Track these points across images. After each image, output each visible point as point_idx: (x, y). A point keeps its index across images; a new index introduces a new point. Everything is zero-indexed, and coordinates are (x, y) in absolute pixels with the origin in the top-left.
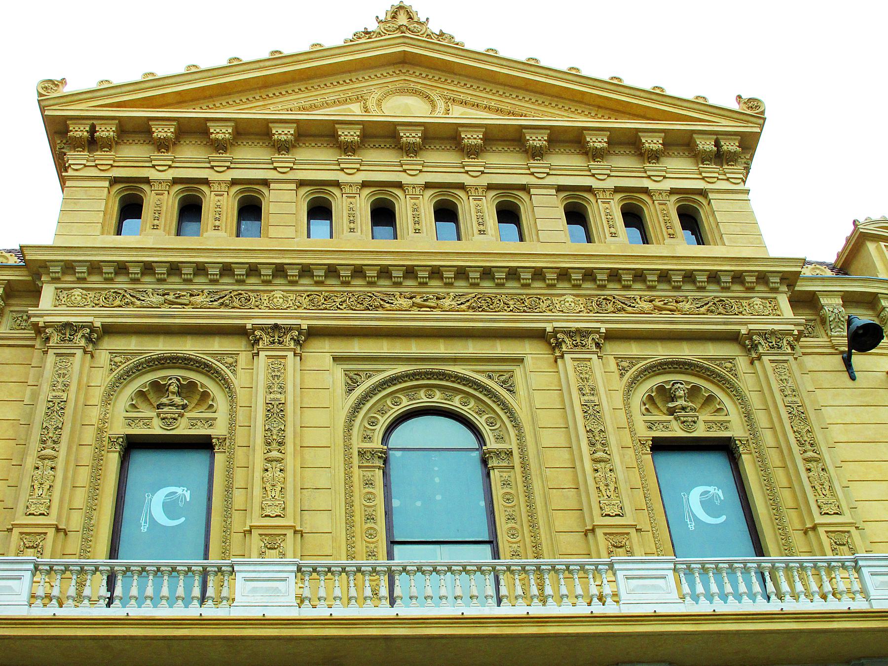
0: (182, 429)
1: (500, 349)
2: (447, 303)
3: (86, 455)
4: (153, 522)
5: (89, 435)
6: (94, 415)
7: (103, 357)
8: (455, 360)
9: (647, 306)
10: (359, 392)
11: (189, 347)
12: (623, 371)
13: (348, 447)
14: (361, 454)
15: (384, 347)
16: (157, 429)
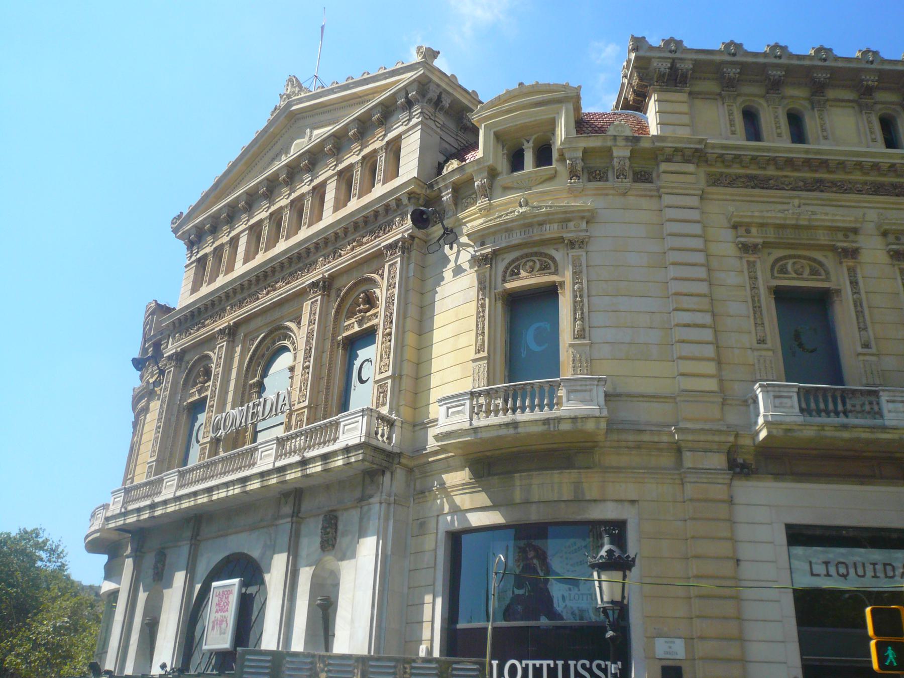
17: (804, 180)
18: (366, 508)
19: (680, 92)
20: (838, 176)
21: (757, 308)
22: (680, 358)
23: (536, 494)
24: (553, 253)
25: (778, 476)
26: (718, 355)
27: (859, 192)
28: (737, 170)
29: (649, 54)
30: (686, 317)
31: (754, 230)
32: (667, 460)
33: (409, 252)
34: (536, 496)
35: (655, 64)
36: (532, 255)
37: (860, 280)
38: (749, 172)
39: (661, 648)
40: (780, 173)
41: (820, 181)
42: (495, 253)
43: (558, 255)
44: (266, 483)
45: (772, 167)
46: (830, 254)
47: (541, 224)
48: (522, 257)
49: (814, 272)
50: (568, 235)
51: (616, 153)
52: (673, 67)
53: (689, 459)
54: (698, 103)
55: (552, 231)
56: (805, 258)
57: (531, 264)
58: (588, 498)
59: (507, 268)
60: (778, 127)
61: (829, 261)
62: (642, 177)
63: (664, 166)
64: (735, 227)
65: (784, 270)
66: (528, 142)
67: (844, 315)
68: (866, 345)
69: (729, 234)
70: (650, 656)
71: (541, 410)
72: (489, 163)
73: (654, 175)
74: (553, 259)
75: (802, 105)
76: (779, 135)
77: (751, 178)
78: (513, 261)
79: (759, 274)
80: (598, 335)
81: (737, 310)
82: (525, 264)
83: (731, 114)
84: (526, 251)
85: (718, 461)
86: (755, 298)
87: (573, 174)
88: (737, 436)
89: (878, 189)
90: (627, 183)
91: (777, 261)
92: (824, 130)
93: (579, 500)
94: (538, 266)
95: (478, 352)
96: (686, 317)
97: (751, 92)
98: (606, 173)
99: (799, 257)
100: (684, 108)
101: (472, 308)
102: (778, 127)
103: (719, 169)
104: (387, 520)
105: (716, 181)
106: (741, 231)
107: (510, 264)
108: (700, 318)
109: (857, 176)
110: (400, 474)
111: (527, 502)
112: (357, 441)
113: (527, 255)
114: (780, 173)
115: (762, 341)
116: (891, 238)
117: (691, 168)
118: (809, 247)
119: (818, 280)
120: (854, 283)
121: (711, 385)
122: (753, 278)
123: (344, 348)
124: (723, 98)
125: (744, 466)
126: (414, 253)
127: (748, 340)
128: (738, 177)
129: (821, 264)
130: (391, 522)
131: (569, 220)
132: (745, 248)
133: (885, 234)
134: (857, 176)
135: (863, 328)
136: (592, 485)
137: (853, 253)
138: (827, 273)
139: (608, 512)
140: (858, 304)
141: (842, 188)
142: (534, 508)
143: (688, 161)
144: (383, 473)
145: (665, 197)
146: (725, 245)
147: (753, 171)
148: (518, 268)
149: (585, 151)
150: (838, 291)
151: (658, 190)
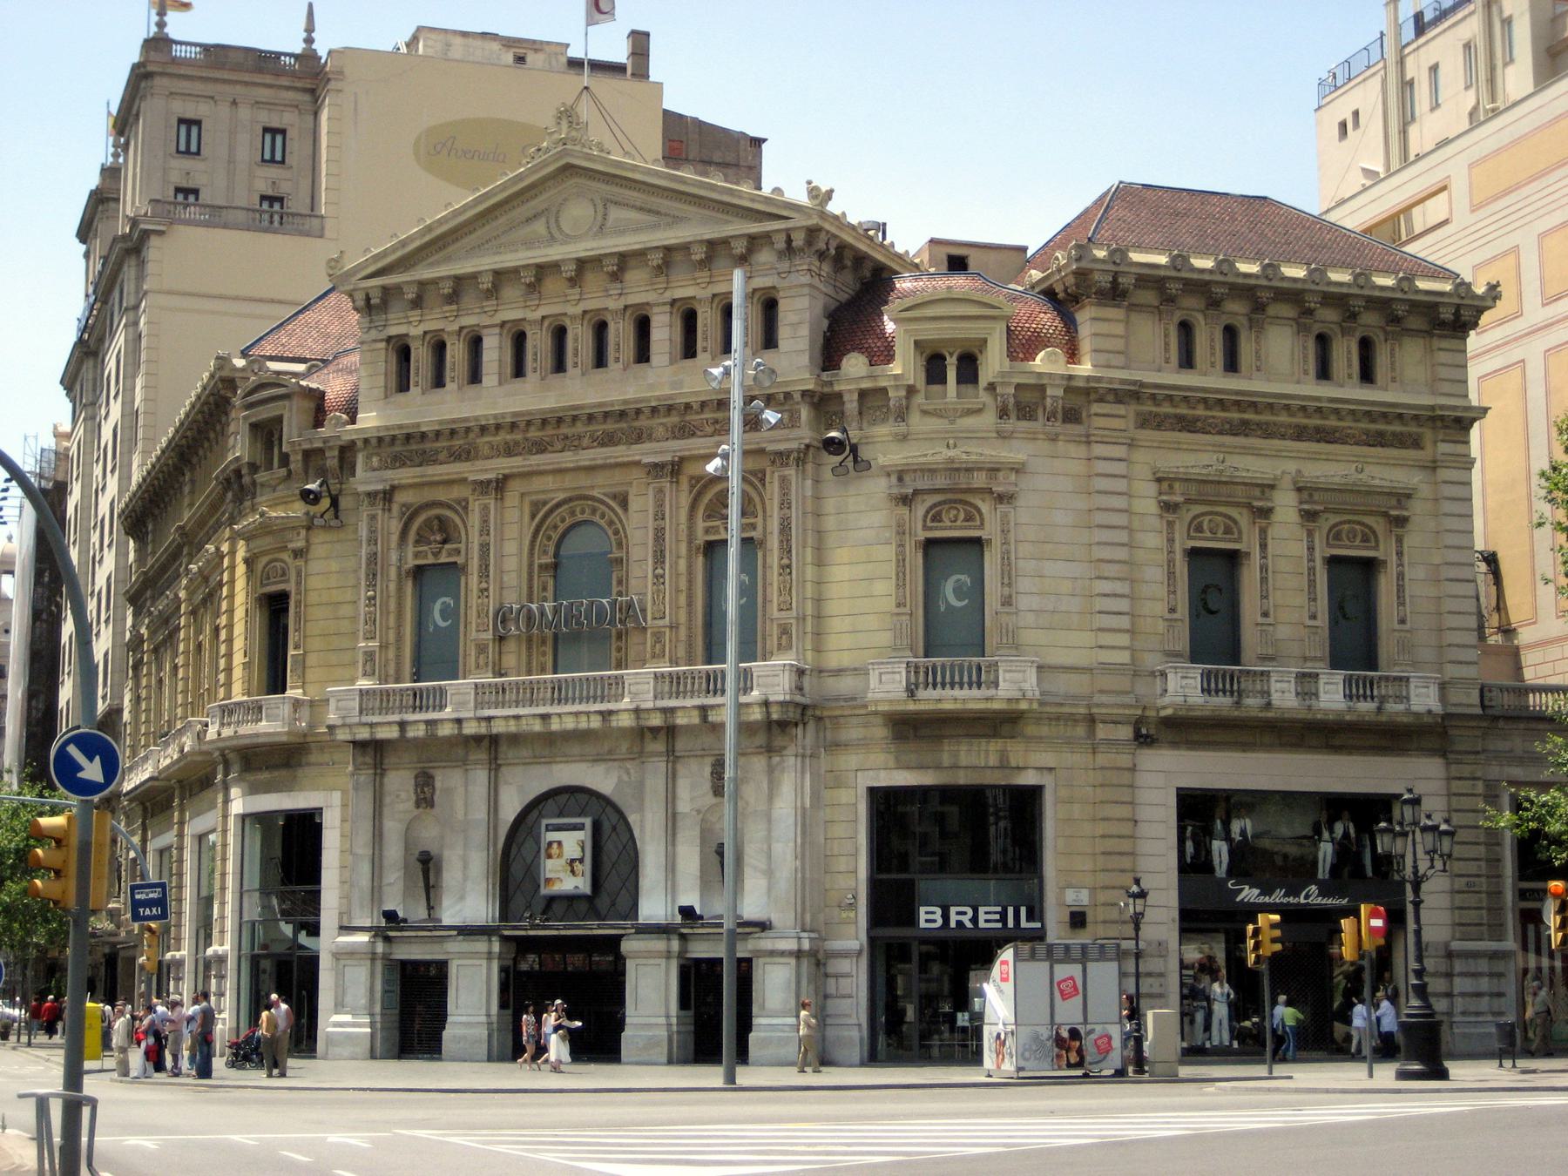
0: (443, 559)
1: (618, 476)
2: (586, 442)
3: (392, 586)
4: (436, 626)
5: (393, 572)
6: (394, 557)
7: (395, 508)
8: (593, 487)
9: (709, 429)
10: (537, 520)
11: (441, 495)
12: (692, 487)
13: (531, 565)
14: (540, 566)
15: (549, 482)
16: (430, 560)
17: (1229, 422)
18: (776, 759)
19: (1118, 306)
20: (1266, 417)
21: (1171, 574)
22: (1099, 630)
23: (964, 760)
24: (980, 504)
25: (1175, 745)
26: (1133, 624)
27: (1283, 437)
28: (1166, 409)
29: (1090, 266)
30: (1106, 586)
31: (1177, 485)
32: (1081, 731)
33: (804, 463)
34: (964, 761)
35: (1096, 276)
36: (955, 501)
37: (1270, 542)
38: (1178, 411)
39: (1071, 896)
40: (1209, 413)
41: (1245, 423)
42: (916, 492)
43: (985, 507)
44: (643, 723)
45: (1201, 406)
46: (1245, 511)
47: (967, 470)
48: (944, 502)
49: (1228, 531)
50: (998, 489)
51: (1049, 392)
52: (1115, 282)
53: (1102, 731)
54: (1134, 317)
55: (979, 480)
56: (1221, 514)
57: (954, 512)
58: (1013, 764)
59: (928, 512)
60: (1213, 354)
61: (1243, 518)
62: (1071, 416)
63: (1096, 408)
64: (1159, 480)
65: (1199, 529)
66: (951, 354)
67: (1250, 577)
68: (1265, 614)
69: (1152, 489)
70: (1061, 904)
71: (979, 687)
72: (911, 382)
73: (1084, 415)
74: (979, 511)
75: (1241, 323)
76: (1213, 365)
77: (1180, 419)
78: (935, 505)
79: (1177, 536)
80: (1023, 602)
81: (1154, 575)
82: (948, 511)
83: (1166, 336)
84: (950, 496)
85: (1126, 732)
86: (1171, 562)
87: (1003, 413)
88: (1145, 708)
89: (1300, 434)
90: (1058, 427)
91: (1195, 518)
92: (1258, 358)
93: (1004, 766)
94: (962, 516)
95: (899, 605)
96: (1106, 586)
97: (1191, 305)
98: (1035, 411)
99: (1217, 514)
100: (1119, 329)
101: (890, 552)
102: (1213, 354)
103: (1149, 407)
104: (803, 773)
105: (1144, 422)
106: (1165, 485)
107: (931, 508)
108: (1120, 587)
109: (1283, 418)
110: (811, 726)
111: (955, 767)
112: (781, 698)
113: (951, 501)
114: (1209, 413)
115: (1172, 610)
116: (1305, 495)
117: (1120, 409)
118: (1228, 504)
119: (1230, 541)
120: (1263, 546)
121: (1124, 657)
122: (1171, 540)
123: (705, 555)
124: (1160, 313)
125: (1147, 736)
126: (809, 467)
127: (1160, 608)
128: (1167, 416)
129: (1235, 522)
130: (808, 776)
131: (998, 470)
132: (1168, 507)
133: (1299, 490)
134: (1283, 418)
135: (1264, 597)
136: (1017, 752)
137: (1266, 513)
138: (1240, 532)
139: (1028, 779)
140: (1264, 569)
141: (1268, 432)
142: (961, 773)
143: (1119, 401)
144: (796, 725)
145: (1095, 446)
146: (1147, 503)
147: (1183, 410)
148: (939, 514)
149: (1018, 387)
150: (1248, 554)
151: (1088, 436)
